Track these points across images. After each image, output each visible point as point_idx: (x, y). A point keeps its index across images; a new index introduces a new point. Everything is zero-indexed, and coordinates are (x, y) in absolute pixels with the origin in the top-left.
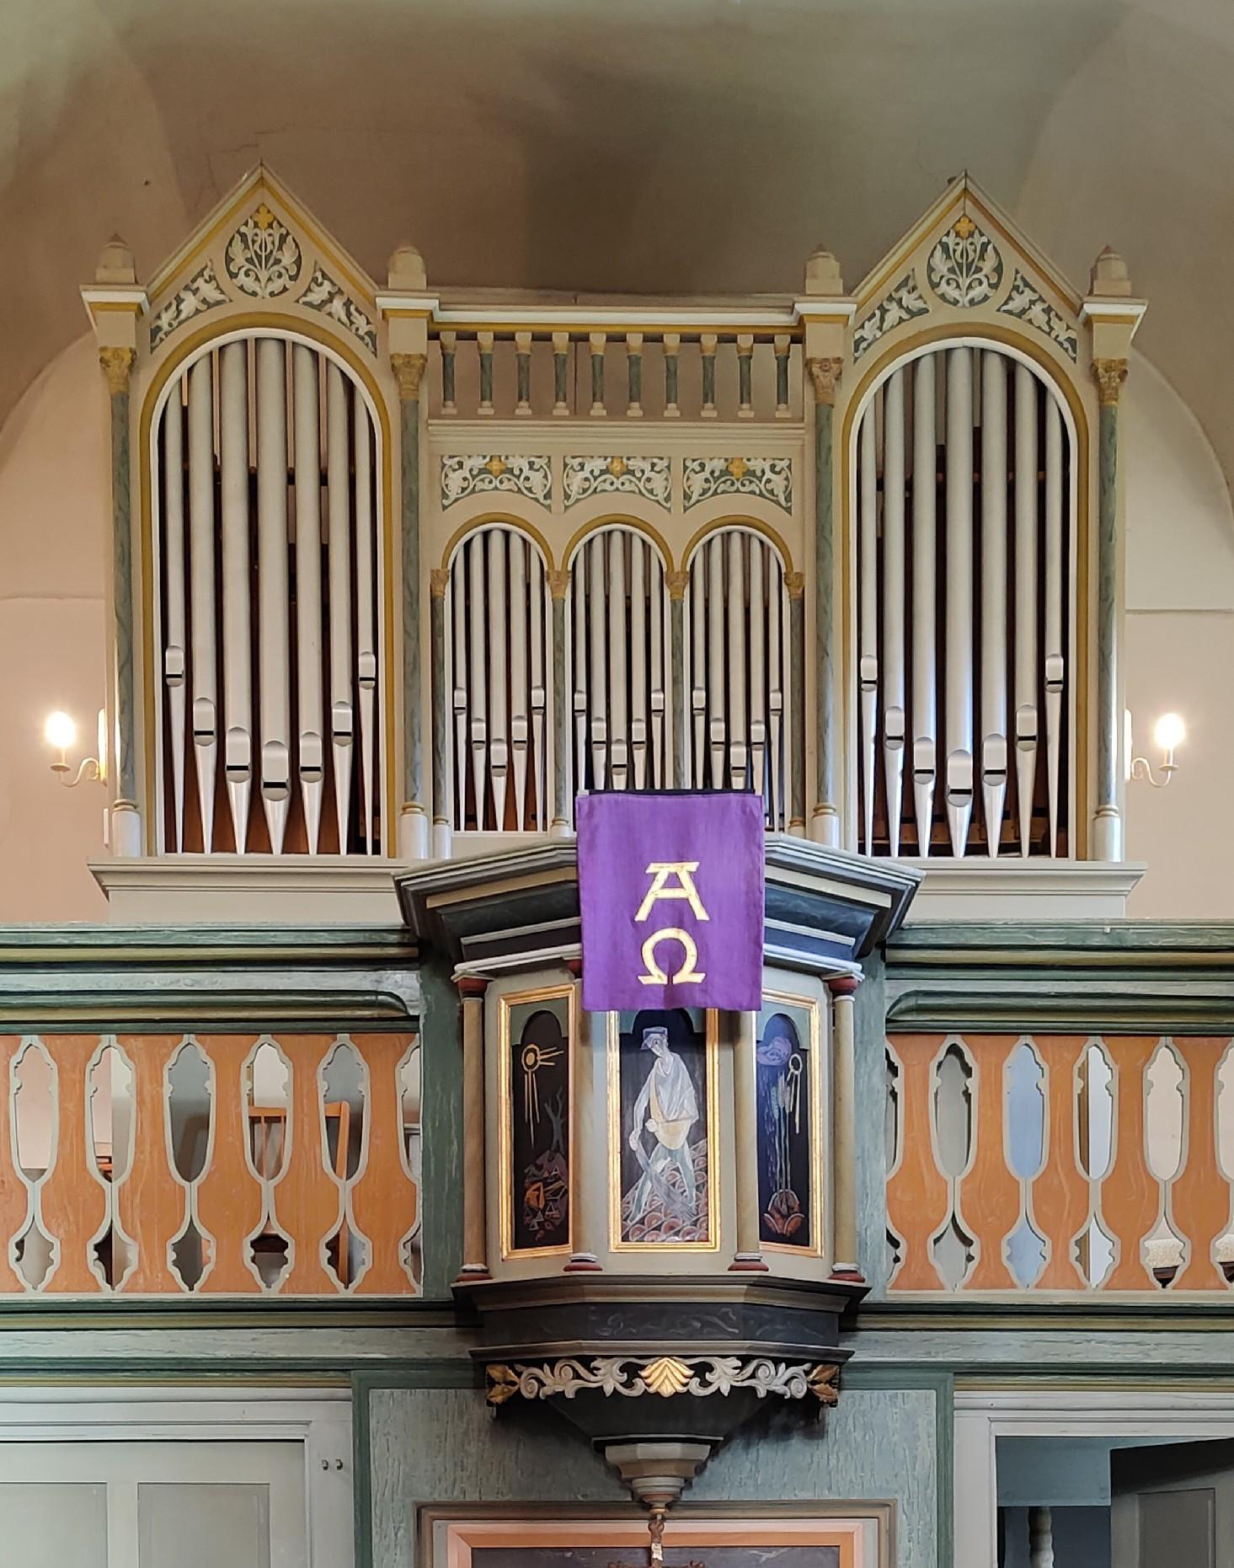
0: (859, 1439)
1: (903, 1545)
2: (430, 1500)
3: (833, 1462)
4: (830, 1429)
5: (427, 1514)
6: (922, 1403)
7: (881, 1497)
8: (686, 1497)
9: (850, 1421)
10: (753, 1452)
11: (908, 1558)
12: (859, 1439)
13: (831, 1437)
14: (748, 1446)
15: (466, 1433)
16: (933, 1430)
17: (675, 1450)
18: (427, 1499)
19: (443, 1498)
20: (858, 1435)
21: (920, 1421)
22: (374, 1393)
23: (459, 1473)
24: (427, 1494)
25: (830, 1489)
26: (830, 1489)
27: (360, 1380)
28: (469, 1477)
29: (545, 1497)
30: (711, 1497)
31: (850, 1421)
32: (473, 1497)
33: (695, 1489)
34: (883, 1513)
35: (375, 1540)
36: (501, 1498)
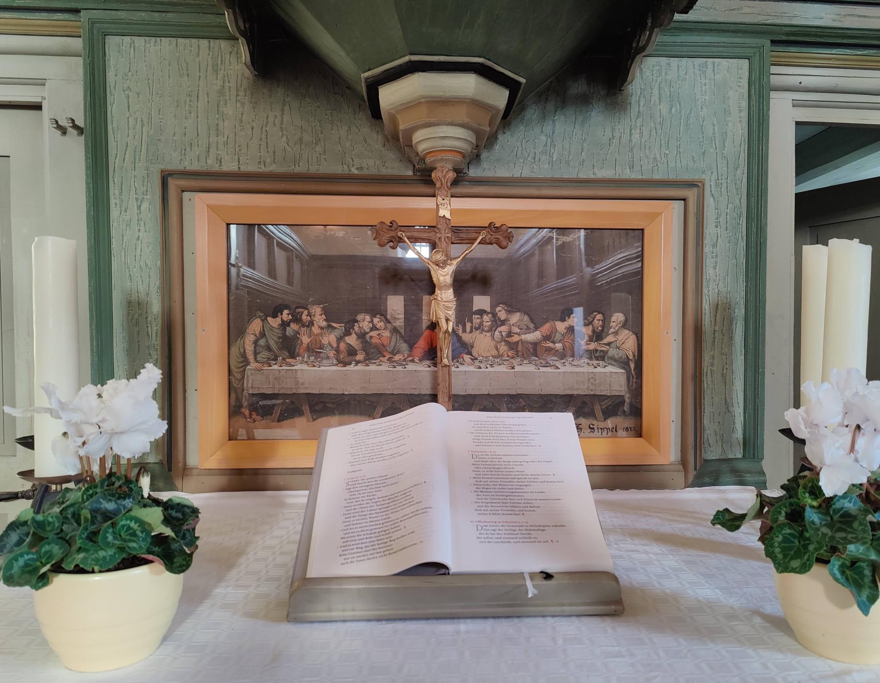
0: (665, 111)
1: (710, 230)
2: (181, 167)
3: (636, 137)
4: (634, 100)
5: (172, 183)
6: (731, 74)
7: (686, 177)
8: (473, 172)
9: (656, 92)
10: (548, 128)
11: (715, 245)
12: (665, 111)
13: (634, 110)
14: (543, 118)
15: (221, 92)
16: (745, 104)
17: (467, 84)
18: (170, 167)
19: (196, 167)
20: (664, 108)
21: (731, 93)
22: (112, 42)
23: (213, 139)
24: (174, 162)
25: (632, 167)
26: (632, 167)
27: (92, 23)
28: (226, 144)
29: (314, 169)
30: (502, 172)
31: (656, 92)
32: (230, 166)
33: (485, 165)
34: (691, 194)
35: (114, 213)
36: (263, 169)
